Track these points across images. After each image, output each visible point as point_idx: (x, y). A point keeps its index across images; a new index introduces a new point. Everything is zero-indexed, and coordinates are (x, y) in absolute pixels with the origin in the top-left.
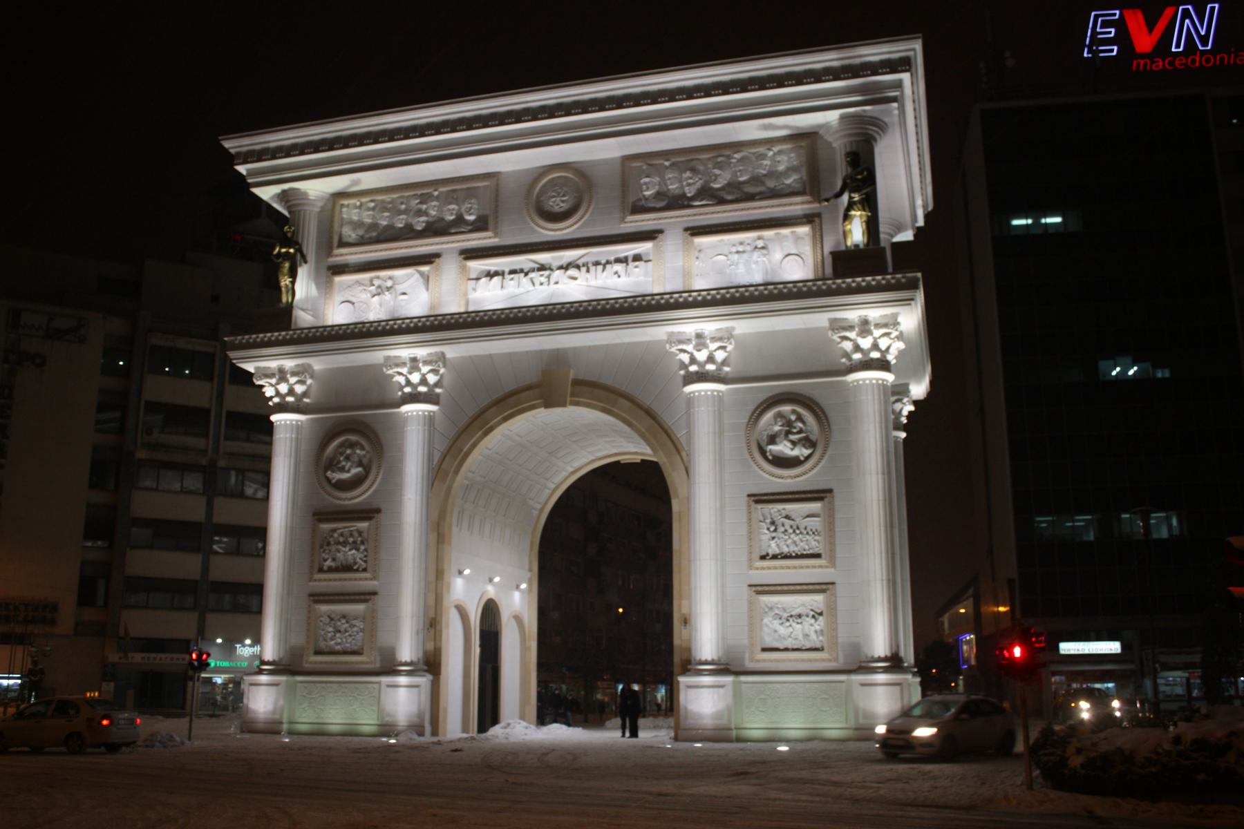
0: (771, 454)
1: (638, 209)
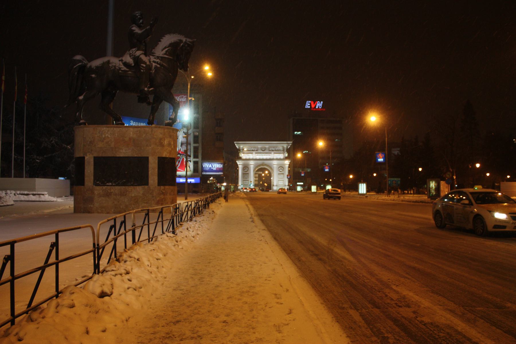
1: (270, 151)
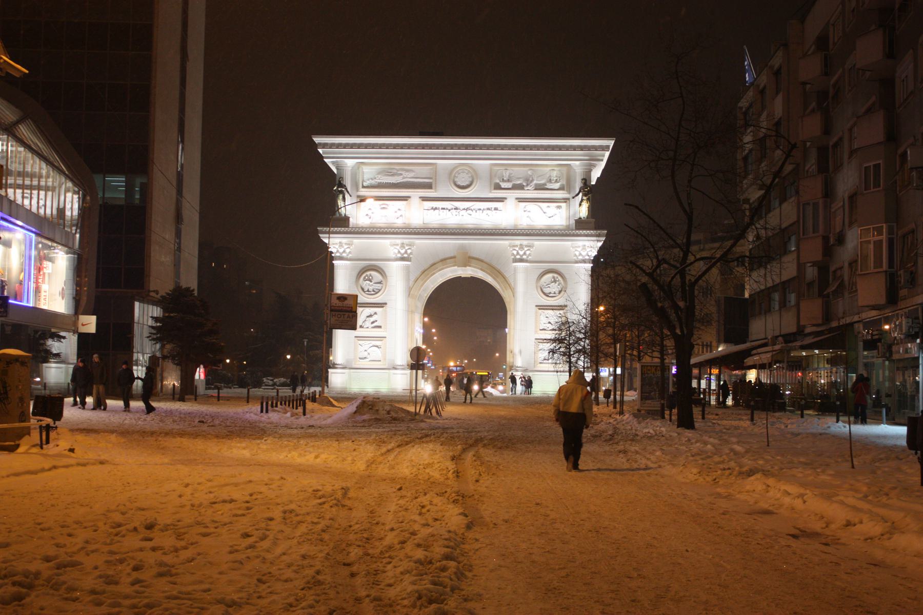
1: (498, 187)
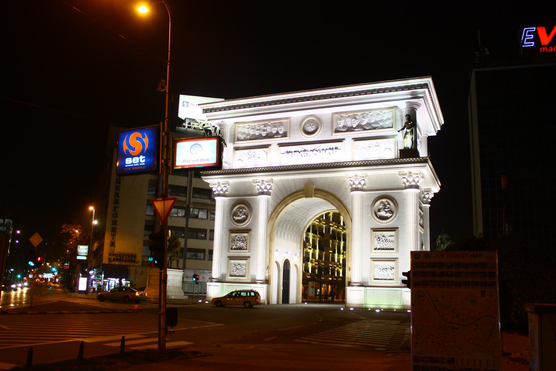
0: (379, 215)
1: (337, 131)
